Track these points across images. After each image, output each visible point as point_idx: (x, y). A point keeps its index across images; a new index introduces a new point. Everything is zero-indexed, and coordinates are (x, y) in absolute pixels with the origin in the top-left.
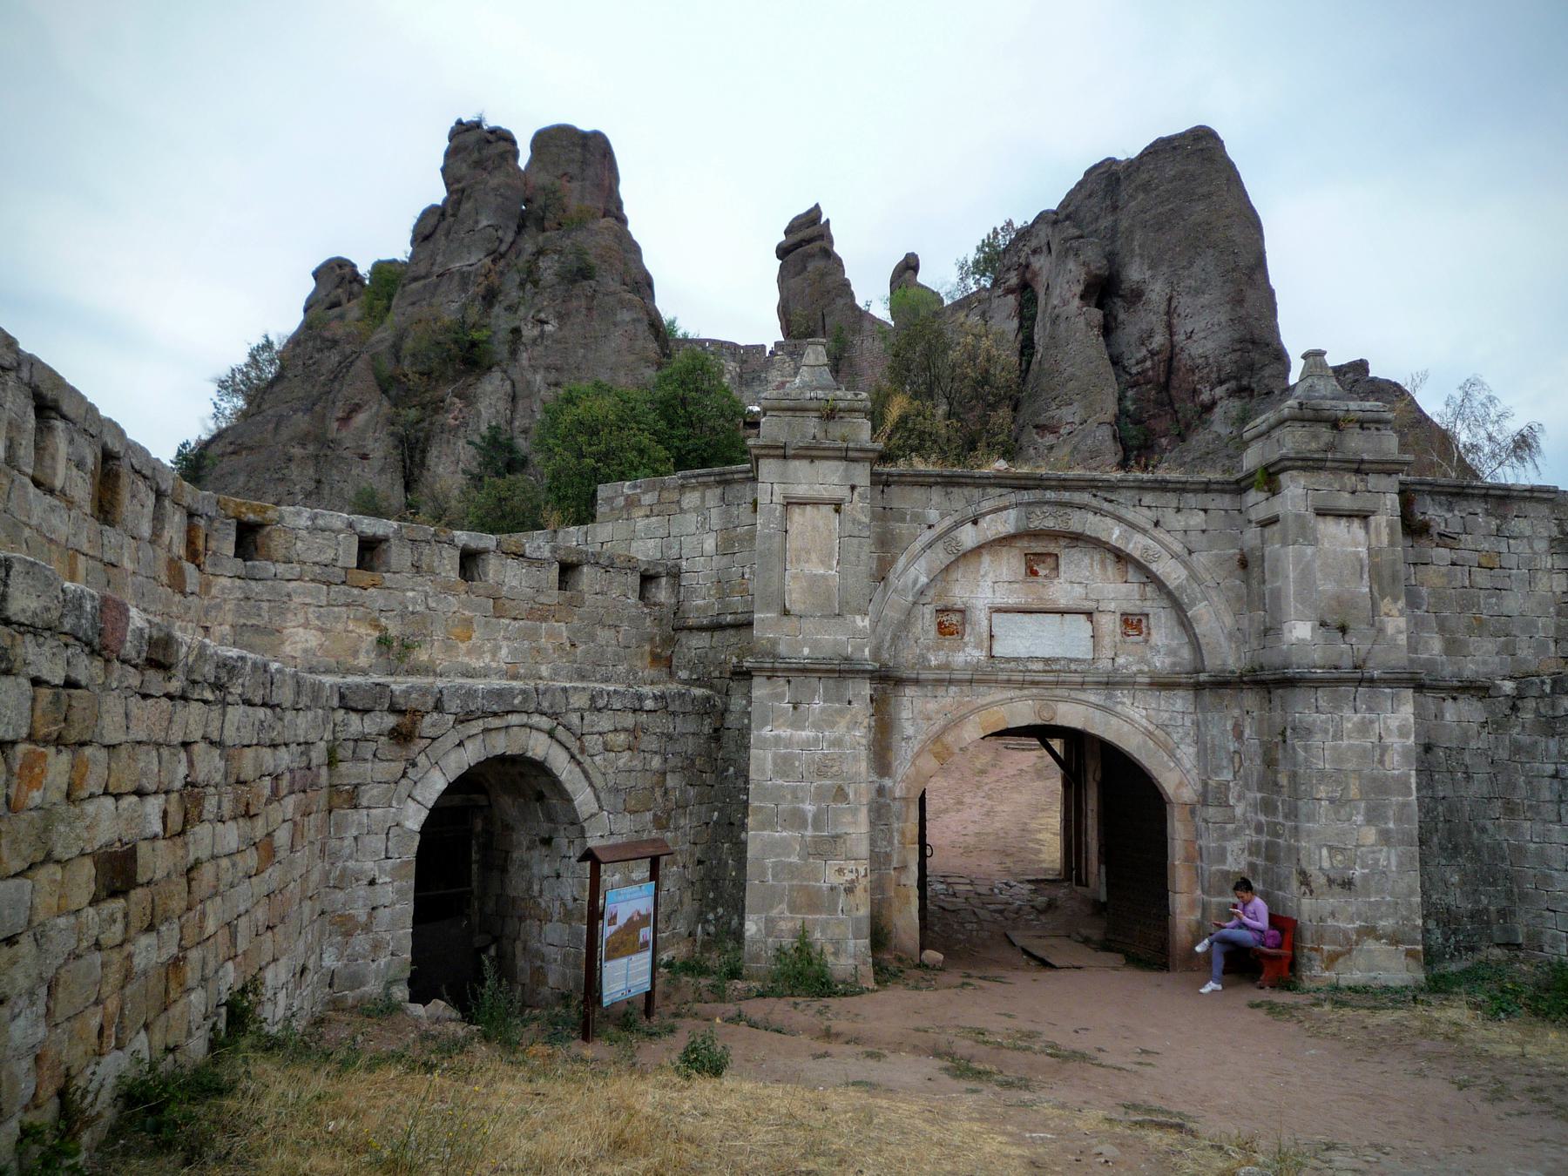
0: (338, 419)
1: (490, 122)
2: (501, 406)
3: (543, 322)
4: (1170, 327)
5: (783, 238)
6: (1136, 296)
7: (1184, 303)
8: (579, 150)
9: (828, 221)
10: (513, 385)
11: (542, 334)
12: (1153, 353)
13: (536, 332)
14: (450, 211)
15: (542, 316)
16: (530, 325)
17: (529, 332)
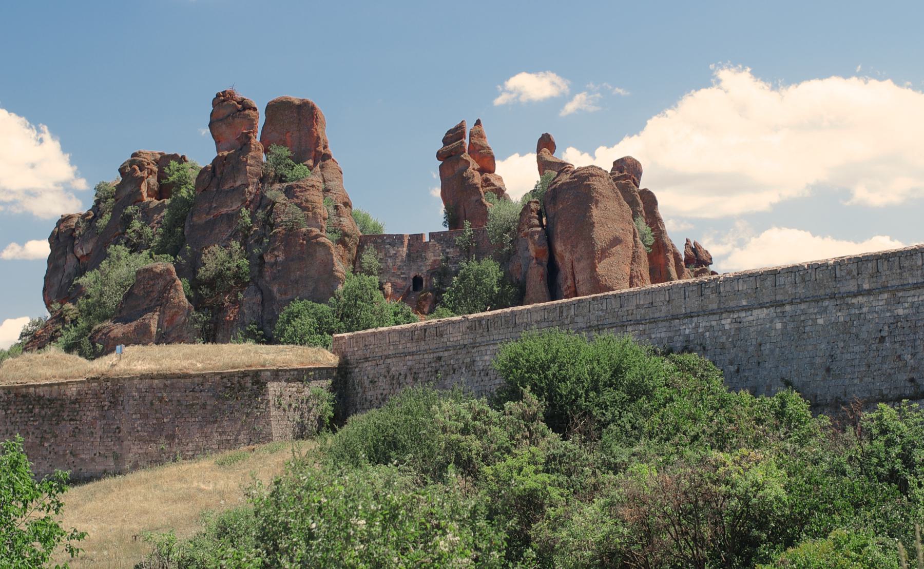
0: (167, 321)
1: (240, 94)
2: (255, 308)
3: (276, 256)
4: (573, 274)
5: (441, 145)
6: (562, 258)
7: (575, 264)
8: (295, 115)
9: (478, 123)
10: (262, 293)
11: (276, 263)
12: (569, 287)
13: (273, 260)
14: (218, 171)
15: (276, 253)
16: (269, 257)
17: (268, 258)
